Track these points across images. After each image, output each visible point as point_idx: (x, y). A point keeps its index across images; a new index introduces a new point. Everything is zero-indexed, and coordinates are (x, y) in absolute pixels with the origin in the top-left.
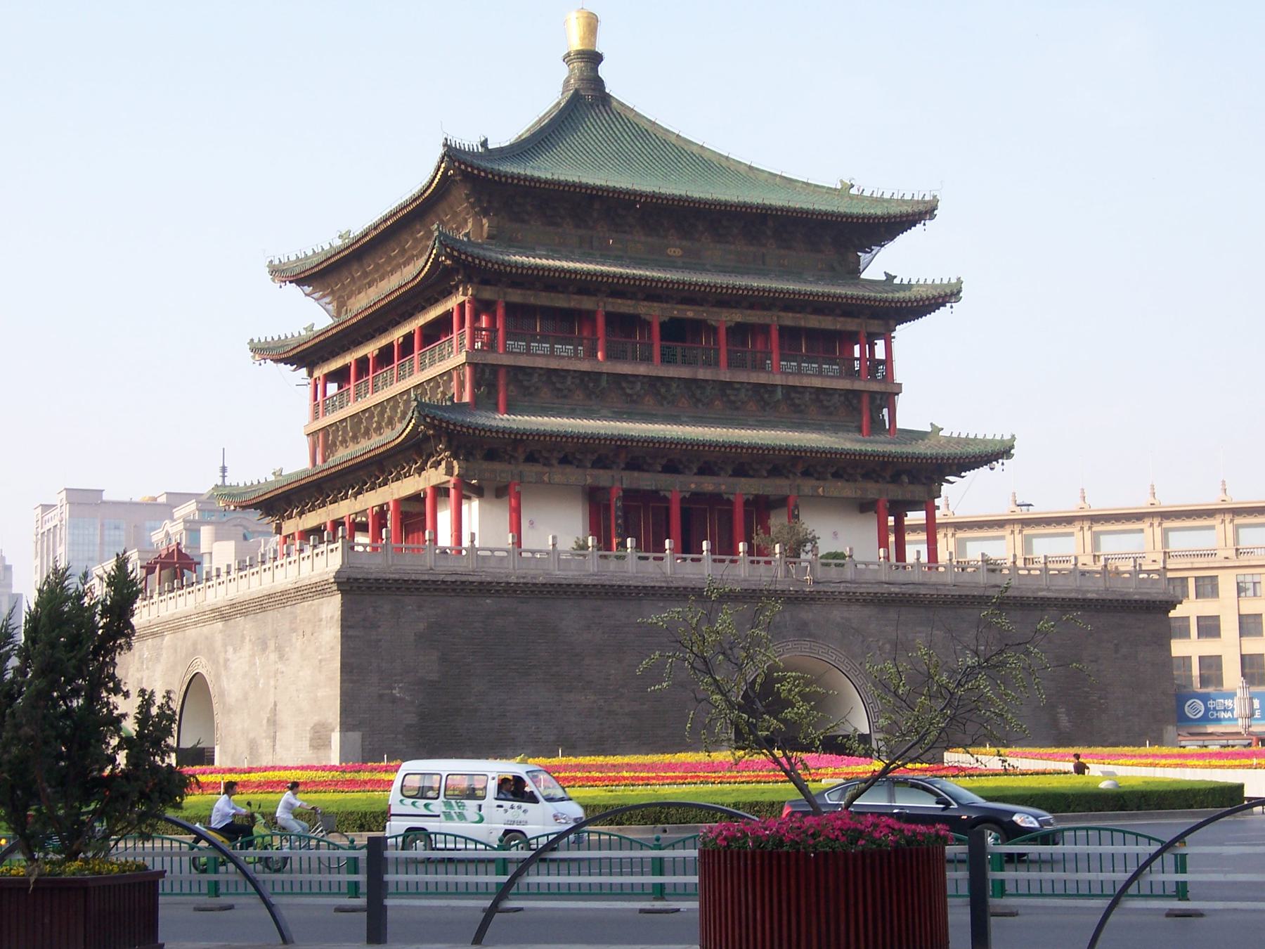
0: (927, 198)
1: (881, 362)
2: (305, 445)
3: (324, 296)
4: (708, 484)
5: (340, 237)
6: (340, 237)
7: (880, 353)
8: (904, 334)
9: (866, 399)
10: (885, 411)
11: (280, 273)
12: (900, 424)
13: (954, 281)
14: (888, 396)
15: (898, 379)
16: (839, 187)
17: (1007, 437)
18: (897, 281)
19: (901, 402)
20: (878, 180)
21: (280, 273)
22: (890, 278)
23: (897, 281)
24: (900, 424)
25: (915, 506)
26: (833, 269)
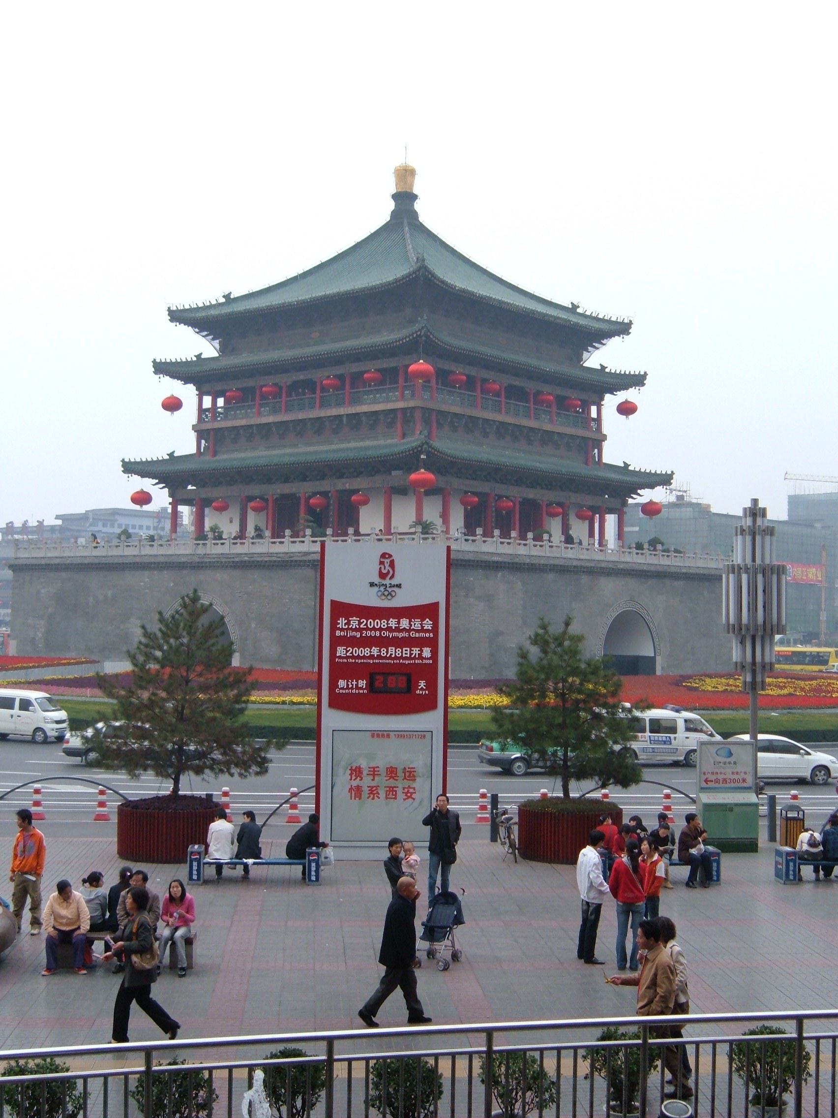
0: (626, 321)
1: (594, 420)
2: (193, 436)
3: (207, 335)
4: (531, 494)
5: (224, 297)
6: (224, 297)
7: (594, 413)
8: (611, 402)
9: (590, 443)
10: (596, 451)
11: (177, 316)
12: (606, 459)
13: (642, 373)
14: (598, 441)
15: (605, 430)
16: (570, 306)
17: (669, 472)
18: (607, 370)
19: (605, 445)
20: (596, 304)
21: (177, 316)
22: (603, 368)
23: (607, 370)
24: (606, 459)
25: (611, 511)
26: (571, 360)
